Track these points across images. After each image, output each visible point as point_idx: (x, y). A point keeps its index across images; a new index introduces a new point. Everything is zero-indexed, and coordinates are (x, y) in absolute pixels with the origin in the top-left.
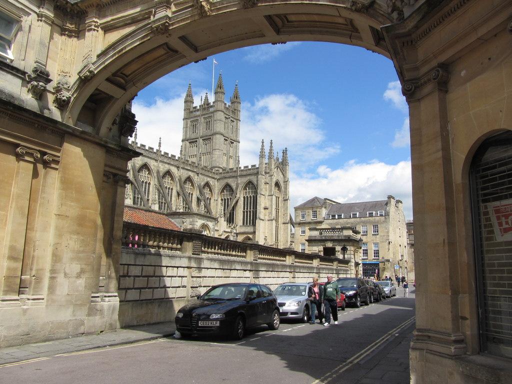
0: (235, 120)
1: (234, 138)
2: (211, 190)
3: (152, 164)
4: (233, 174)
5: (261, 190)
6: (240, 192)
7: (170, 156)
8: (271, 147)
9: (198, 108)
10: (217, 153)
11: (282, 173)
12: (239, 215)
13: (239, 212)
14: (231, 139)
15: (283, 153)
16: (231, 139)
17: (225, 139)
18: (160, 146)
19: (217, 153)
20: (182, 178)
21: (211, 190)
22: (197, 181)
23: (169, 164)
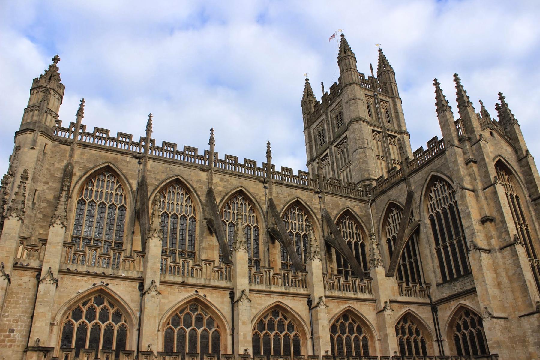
0: (389, 100)
2: (359, 227)
3: (194, 178)
4: (400, 176)
8: (459, 87)
9: (321, 102)
11: (507, 141)
14: (388, 130)
15: (498, 109)
16: (388, 130)
17: (373, 131)
20: (275, 202)
21: (359, 227)
22: (322, 210)
23: (239, 175)
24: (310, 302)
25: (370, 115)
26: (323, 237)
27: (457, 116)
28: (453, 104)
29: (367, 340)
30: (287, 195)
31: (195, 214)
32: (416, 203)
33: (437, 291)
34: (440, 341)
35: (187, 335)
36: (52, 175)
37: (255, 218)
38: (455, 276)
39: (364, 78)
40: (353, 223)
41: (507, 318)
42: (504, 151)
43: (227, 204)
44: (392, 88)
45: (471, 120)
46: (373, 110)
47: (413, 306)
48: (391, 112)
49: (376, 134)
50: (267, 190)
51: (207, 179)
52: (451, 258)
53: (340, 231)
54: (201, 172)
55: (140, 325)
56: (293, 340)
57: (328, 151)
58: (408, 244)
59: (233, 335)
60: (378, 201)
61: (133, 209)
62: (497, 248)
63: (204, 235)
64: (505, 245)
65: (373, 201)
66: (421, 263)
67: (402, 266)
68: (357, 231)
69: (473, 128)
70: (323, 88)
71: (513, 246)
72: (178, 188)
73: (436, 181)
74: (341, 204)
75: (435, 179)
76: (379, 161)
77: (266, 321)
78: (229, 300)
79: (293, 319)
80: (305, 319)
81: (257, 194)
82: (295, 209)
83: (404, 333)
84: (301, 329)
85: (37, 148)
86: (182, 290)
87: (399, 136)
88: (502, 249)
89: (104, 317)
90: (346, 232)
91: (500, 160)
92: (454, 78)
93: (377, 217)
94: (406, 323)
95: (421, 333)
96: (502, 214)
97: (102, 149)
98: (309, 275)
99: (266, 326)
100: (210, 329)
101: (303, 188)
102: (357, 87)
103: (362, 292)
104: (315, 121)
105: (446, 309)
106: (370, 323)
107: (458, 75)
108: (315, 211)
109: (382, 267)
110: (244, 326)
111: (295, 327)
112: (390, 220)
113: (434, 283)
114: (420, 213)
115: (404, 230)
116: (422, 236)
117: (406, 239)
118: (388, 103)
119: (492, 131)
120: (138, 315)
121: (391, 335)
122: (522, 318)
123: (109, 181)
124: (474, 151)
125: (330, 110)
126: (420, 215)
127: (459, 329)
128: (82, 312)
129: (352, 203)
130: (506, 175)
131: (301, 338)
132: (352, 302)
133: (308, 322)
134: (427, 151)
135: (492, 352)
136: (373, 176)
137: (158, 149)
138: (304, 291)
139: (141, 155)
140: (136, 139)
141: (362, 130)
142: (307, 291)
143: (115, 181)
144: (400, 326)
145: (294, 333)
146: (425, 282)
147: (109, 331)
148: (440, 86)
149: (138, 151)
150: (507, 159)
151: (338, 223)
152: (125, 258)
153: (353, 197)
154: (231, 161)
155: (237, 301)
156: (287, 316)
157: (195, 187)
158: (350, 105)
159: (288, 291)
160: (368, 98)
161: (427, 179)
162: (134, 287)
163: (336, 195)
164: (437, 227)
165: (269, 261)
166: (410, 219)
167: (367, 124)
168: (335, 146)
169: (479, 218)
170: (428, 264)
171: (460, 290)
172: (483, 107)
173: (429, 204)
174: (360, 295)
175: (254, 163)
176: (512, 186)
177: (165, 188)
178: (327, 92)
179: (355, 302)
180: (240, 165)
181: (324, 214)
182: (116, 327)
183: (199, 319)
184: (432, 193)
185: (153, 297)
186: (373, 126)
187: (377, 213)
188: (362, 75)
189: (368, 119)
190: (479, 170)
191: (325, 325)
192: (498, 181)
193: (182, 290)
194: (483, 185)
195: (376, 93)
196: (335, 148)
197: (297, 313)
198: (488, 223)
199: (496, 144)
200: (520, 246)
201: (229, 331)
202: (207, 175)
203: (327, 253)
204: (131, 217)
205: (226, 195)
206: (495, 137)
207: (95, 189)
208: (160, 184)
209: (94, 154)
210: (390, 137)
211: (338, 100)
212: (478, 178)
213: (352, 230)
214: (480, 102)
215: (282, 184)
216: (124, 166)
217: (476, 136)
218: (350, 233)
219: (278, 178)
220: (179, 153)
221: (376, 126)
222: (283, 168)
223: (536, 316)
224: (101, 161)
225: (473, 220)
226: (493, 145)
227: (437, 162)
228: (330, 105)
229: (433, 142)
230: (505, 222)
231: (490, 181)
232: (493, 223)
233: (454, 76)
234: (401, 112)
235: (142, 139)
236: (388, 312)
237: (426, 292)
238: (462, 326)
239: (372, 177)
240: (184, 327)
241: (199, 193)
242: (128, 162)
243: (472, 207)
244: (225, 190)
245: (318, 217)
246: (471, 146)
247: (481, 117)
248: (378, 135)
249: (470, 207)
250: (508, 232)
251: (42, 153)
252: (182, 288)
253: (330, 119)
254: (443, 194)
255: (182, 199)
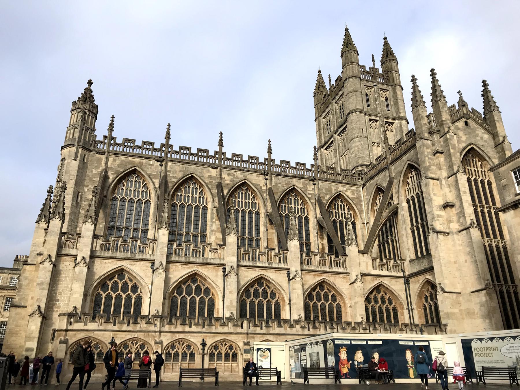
0: (390, 88)
1: (395, 115)
3: (206, 175)
5: (428, 169)
6: (398, 192)
7: (245, 158)
8: (434, 81)
10: (356, 144)
11: (485, 128)
12: (405, 239)
13: (403, 232)
16: (385, 118)
17: (370, 120)
18: (221, 144)
19: (359, 143)
21: (351, 208)
22: (315, 195)
23: (244, 170)
24: (289, 275)
25: (368, 106)
26: (316, 218)
27: (430, 109)
28: (427, 98)
29: (340, 307)
30: (284, 184)
31: (206, 203)
32: (396, 188)
33: (409, 266)
34: (410, 309)
35: (188, 301)
36: (91, 179)
37: (257, 204)
38: (425, 254)
39: (365, 69)
40: (345, 205)
41: (460, 293)
42: (479, 138)
43: (232, 194)
44: (393, 76)
45: (441, 114)
46: (372, 100)
47: (385, 279)
48: (390, 100)
49: (373, 122)
50: (268, 182)
51: (216, 175)
52: (422, 238)
53: (332, 212)
54: (211, 169)
55: (151, 295)
56: (275, 305)
57: (332, 139)
58: (385, 224)
59: (223, 301)
60: (368, 184)
61: (156, 203)
62: (455, 231)
63: (214, 220)
64: (462, 228)
65: (364, 185)
66: (399, 241)
67: (386, 243)
68: (349, 211)
69: (443, 121)
70: (330, 80)
71: (468, 230)
72: (193, 184)
73: (412, 169)
74: (333, 190)
75: (411, 167)
76: (375, 148)
77: (252, 290)
78: (222, 274)
79: (275, 288)
80: (285, 289)
81: (259, 185)
82: (292, 195)
83: (376, 301)
84: (282, 296)
85: (78, 159)
86: (185, 267)
87: (396, 122)
88: (460, 232)
89: (125, 289)
90: (339, 213)
91: (472, 148)
92: (431, 73)
93: (367, 199)
94: (379, 293)
95: (393, 302)
96: (461, 200)
97: (130, 156)
98: (289, 253)
99: (252, 293)
100: (207, 297)
101: (299, 177)
102: (356, 80)
103: (337, 266)
104: (324, 112)
105: (416, 282)
106: (342, 292)
107: (434, 70)
108: (310, 196)
109: (356, 245)
110: (231, 295)
111: (277, 294)
112: (378, 202)
113: (408, 259)
114: (398, 197)
115: (382, 213)
116: (400, 217)
117: (383, 220)
118: (388, 91)
119: (468, 121)
120: (150, 288)
121: (360, 303)
122: (473, 293)
123: (136, 181)
124: (442, 143)
125: (335, 101)
126: (398, 199)
127: (427, 301)
128: (109, 286)
129: (345, 187)
130: (479, 161)
131: (281, 304)
132: (327, 275)
133: (287, 291)
134: (406, 141)
135: (443, 322)
136: (367, 162)
137: (176, 152)
138: (285, 265)
139: (162, 159)
140: (157, 146)
141: (359, 121)
142: (287, 266)
143: (142, 181)
144: (372, 296)
145: (275, 300)
146: (401, 258)
147: (128, 299)
148: (417, 81)
149: (159, 155)
150: (480, 146)
151: (330, 206)
152: (141, 245)
153: (346, 182)
154: (237, 159)
155: (227, 275)
156: (270, 285)
157: (206, 182)
158: (349, 98)
159: (270, 266)
160: (368, 89)
161: (404, 167)
162: (147, 267)
163: (329, 181)
164: (412, 210)
165: (267, 238)
166: (389, 203)
167: (363, 115)
168: (338, 135)
169: (442, 203)
170: (403, 242)
171: (427, 267)
172: (461, 97)
173: (406, 189)
174: (335, 269)
175: (257, 158)
176: (485, 172)
177: (181, 184)
178: (333, 85)
179: (330, 275)
180: (245, 161)
181: (317, 199)
182: (133, 297)
183: (198, 289)
184: (408, 179)
185: (160, 274)
186: (370, 115)
187: (366, 196)
188: (363, 67)
189: (365, 110)
190: (445, 160)
191: (300, 294)
192: (460, 171)
193: (185, 267)
194: (448, 174)
195: (375, 84)
196: (338, 137)
197: (277, 283)
198: (448, 208)
199: (469, 134)
200: (476, 229)
201: (221, 298)
202: (217, 172)
203: (318, 232)
204: (155, 208)
205: (233, 187)
206: (470, 127)
207: (125, 188)
208: (177, 182)
209: (123, 160)
210: (387, 125)
211: (341, 93)
212: (444, 167)
213: (344, 210)
214: (460, 93)
215: (281, 175)
216: (148, 168)
217: (444, 129)
218: (342, 214)
219: (276, 170)
220: (193, 154)
221: (373, 115)
222: (282, 162)
223: (484, 292)
224: (129, 166)
225: (433, 206)
226: (466, 135)
227: (412, 152)
228: (335, 97)
229: (411, 134)
230: (463, 208)
231: (453, 170)
232: (454, 209)
233: (431, 71)
234: (401, 98)
235: (163, 145)
236: (358, 284)
237: (400, 267)
238: (429, 298)
239: (366, 163)
240: (186, 295)
241: (210, 187)
242: (151, 165)
243: (435, 195)
244: (231, 182)
245: (312, 201)
246: (440, 138)
247: (457, 107)
248: (375, 124)
249: (432, 195)
250: (465, 217)
251: (82, 163)
252: (185, 266)
253: (334, 110)
254: (417, 181)
255: (196, 192)
